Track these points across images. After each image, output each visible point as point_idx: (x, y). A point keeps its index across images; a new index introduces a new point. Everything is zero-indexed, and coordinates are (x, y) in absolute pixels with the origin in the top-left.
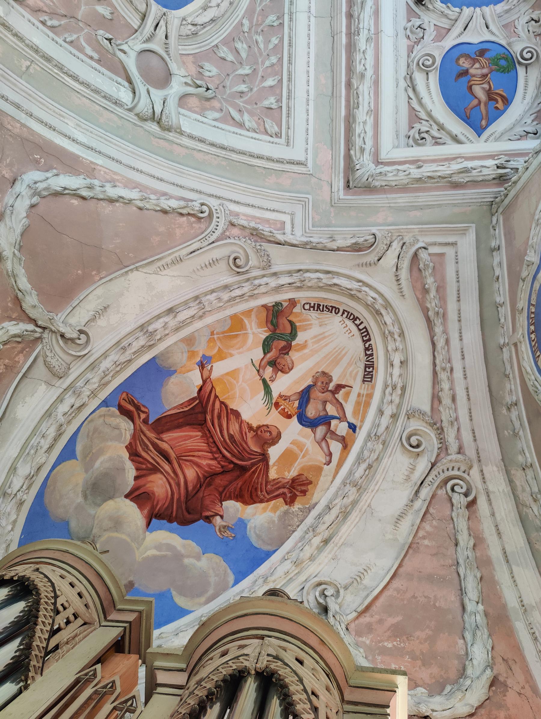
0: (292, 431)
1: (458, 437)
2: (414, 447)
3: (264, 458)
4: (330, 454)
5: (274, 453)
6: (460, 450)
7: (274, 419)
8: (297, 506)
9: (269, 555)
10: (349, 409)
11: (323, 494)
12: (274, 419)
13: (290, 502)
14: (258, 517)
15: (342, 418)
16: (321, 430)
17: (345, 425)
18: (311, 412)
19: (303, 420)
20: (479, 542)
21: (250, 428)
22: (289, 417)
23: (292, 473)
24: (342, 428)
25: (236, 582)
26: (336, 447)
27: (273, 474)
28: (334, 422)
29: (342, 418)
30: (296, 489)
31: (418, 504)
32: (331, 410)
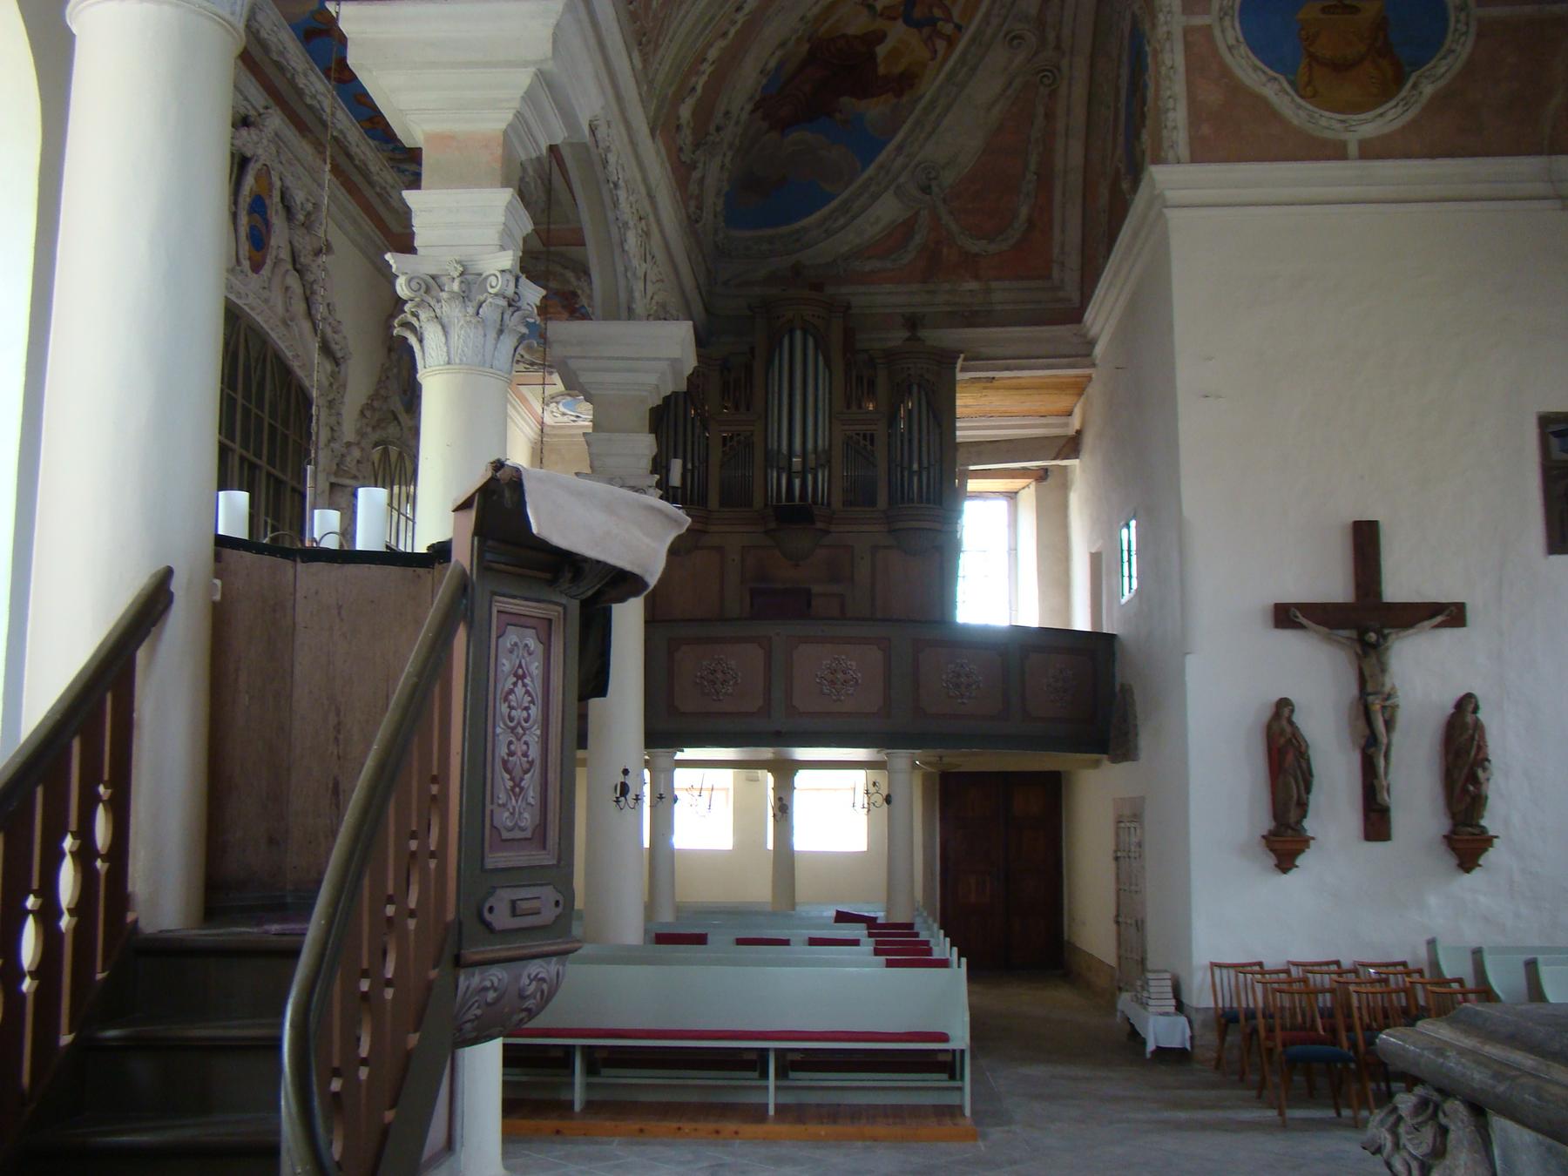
0: (898, 32)
1: (1058, 38)
2: (1014, 39)
3: (872, 57)
4: (935, 52)
5: (881, 51)
6: (1058, 47)
7: (880, 24)
8: (905, 99)
9: (885, 144)
10: (956, 13)
11: (929, 88)
12: (880, 24)
13: (899, 94)
14: (874, 110)
15: (949, 19)
16: (926, 31)
17: (951, 26)
18: (918, 13)
19: (909, 21)
20: (1050, 116)
21: (856, 37)
22: (894, 19)
23: (899, 68)
24: (948, 29)
25: (863, 170)
26: (941, 45)
27: (882, 70)
28: (940, 24)
29: (949, 19)
30: (905, 82)
31: (1009, 92)
32: (937, 12)
